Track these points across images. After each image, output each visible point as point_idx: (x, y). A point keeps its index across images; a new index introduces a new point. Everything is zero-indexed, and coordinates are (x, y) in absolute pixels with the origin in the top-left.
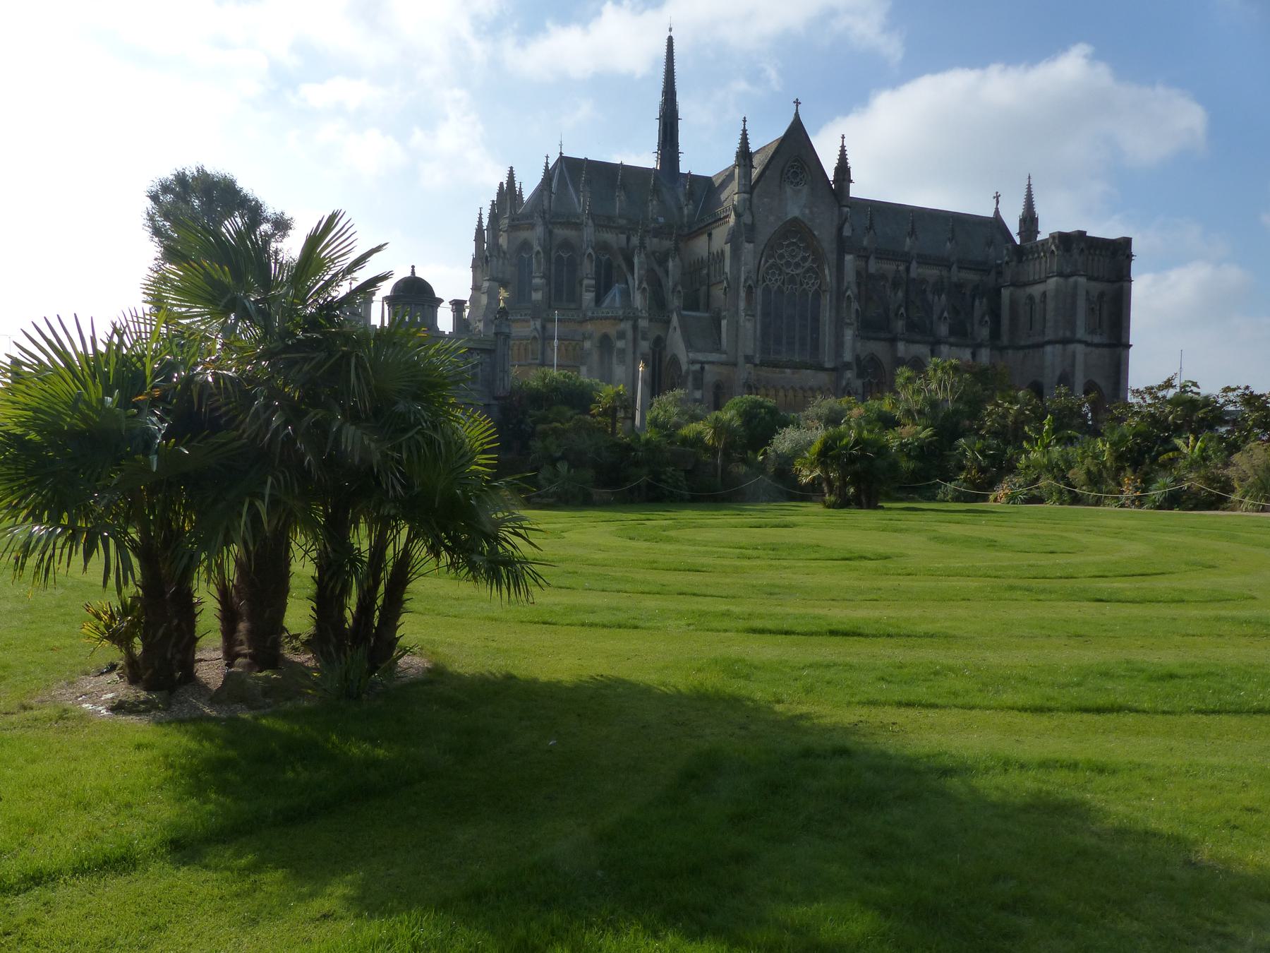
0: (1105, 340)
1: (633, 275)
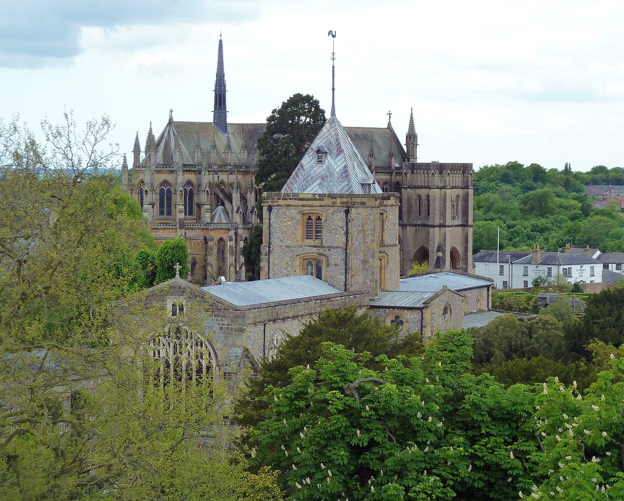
0: (460, 223)
1: (231, 202)
